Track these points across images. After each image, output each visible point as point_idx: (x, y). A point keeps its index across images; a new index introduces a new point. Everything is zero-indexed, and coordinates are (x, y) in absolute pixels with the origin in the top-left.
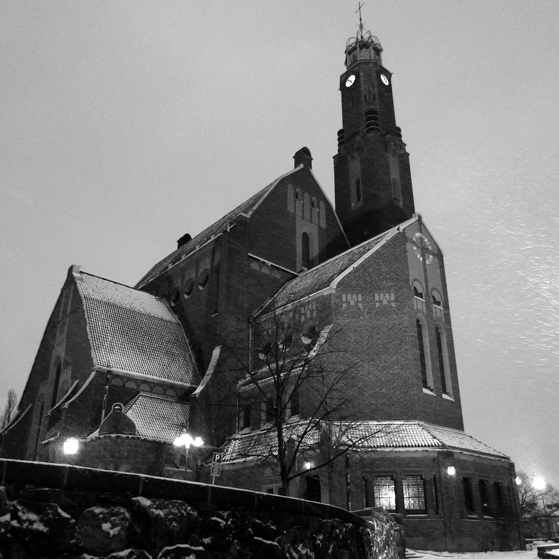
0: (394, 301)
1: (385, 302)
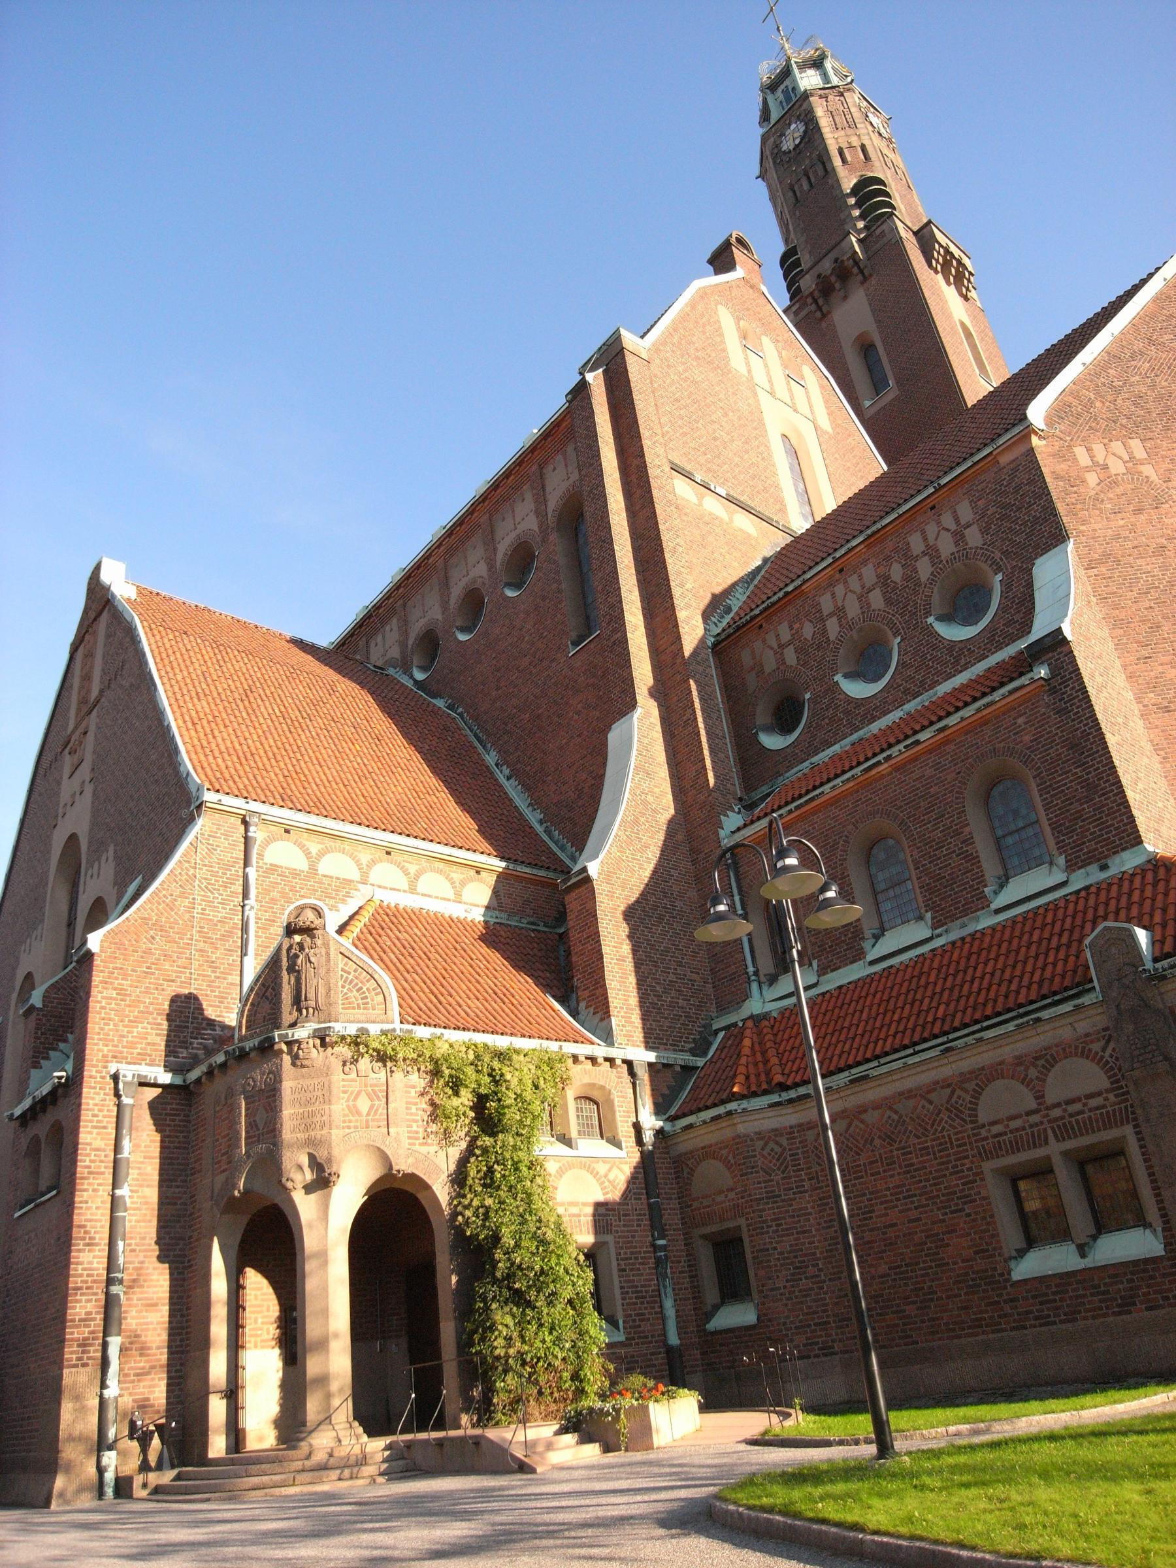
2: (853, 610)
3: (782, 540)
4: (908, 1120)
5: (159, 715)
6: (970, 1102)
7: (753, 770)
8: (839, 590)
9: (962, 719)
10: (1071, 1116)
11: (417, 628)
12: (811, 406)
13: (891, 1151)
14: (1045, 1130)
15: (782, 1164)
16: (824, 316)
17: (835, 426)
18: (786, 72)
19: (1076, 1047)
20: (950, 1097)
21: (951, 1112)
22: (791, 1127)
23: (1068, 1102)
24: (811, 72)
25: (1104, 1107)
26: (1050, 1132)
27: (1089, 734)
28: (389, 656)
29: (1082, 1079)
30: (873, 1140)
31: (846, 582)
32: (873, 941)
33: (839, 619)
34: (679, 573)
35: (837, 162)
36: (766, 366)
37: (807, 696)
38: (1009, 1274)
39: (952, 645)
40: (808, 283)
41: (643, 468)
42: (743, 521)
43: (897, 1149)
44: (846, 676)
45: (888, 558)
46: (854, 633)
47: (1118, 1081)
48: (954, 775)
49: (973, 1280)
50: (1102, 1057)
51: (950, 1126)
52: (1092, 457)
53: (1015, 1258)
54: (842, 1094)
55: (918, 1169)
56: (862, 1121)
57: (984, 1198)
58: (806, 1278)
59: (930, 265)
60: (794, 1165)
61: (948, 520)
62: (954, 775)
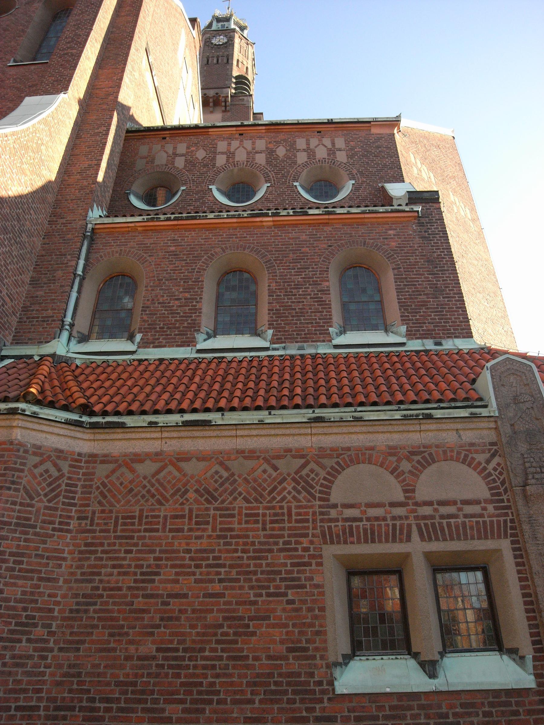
2: (241, 156)
4: (240, 480)
6: (325, 479)
8: (235, 144)
9: (349, 213)
10: (442, 517)
13: (207, 509)
14: (409, 526)
15: (53, 490)
18: (227, 19)
19: (459, 453)
20: (304, 466)
21: (298, 483)
22: (80, 454)
23: (442, 503)
25: (481, 516)
26: (414, 528)
27: (444, 258)
29: (467, 485)
30: (187, 491)
31: (241, 141)
32: (206, 337)
33: (228, 158)
35: (235, 63)
37: (183, 188)
38: (331, 683)
43: (216, 509)
44: (218, 189)
46: (236, 170)
47: (499, 494)
48: (325, 246)
49: (276, 683)
50: (485, 469)
51: (294, 497)
53: (340, 664)
54: (165, 435)
55: (238, 537)
56: (179, 470)
57: (317, 586)
58: (29, 641)
60: (65, 497)
62: (325, 246)
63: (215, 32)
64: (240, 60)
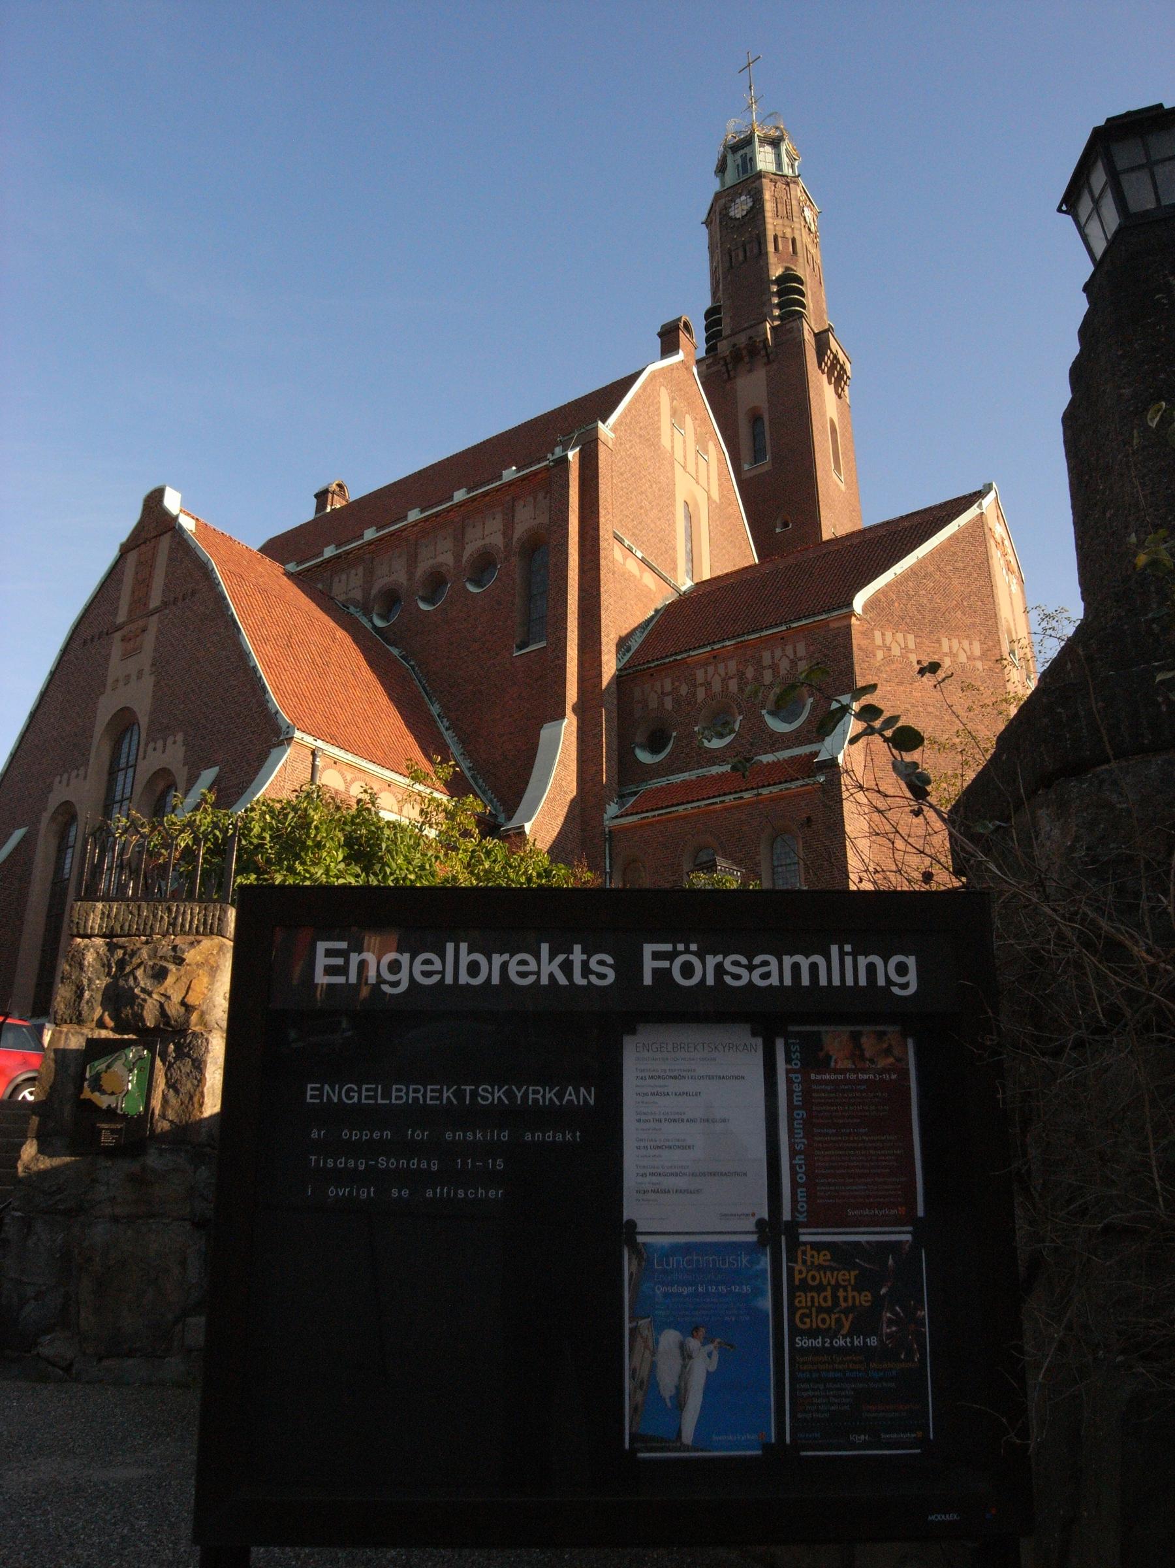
0: (980, 658)
1: (963, 658)
2: (717, 687)
3: (670, 597)
5: (244, 656)
7: (628, 771)
8: (711, 669)
11: (382, 582)
12: (708, 478)
16: (730, 378)
17: (722, 496)
18: (748, 141)
24: (768, 149)
28: (351, 595)
31: (716, 666)
34: (607, 626)
35: (771, 248)
36: (684, 442)
39: (773, 734)
40: (724, 347)
41: (596, 539)
42: (649, 579)
45: (746, 661)
52: (884, 640)
59: (820, 366)
61: (789, 650)
63: (731, 191)
64: (780, 234)
